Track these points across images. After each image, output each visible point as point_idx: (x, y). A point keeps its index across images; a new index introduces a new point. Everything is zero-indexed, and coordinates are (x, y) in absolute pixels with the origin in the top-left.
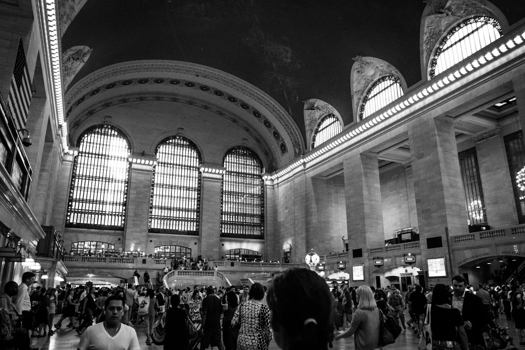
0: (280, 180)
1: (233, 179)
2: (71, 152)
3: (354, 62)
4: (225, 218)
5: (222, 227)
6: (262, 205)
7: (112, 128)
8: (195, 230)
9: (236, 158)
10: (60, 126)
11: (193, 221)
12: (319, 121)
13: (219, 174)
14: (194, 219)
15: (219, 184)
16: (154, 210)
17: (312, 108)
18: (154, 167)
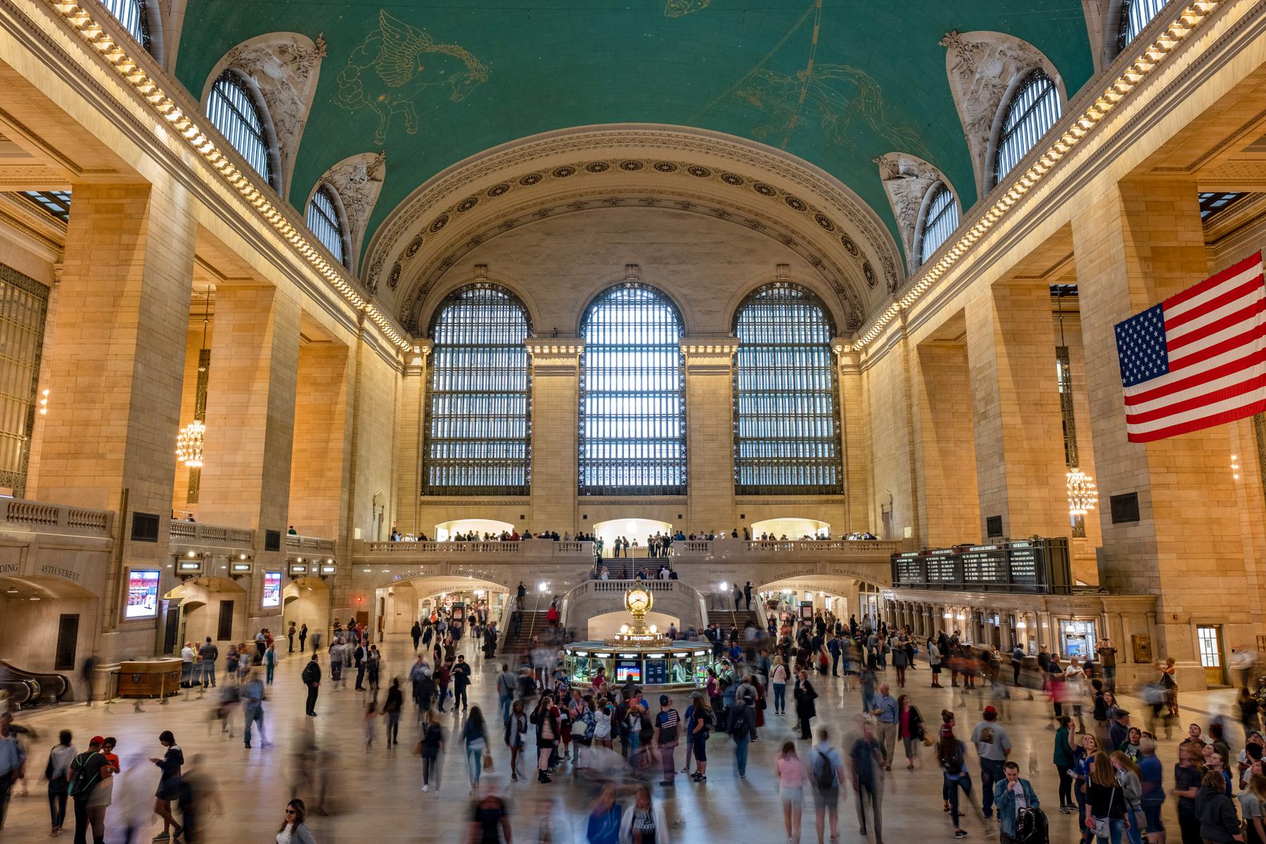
0: (871, 351)
1: (764, 359)
2: (417, 350)
3: (945, 49)
4: (747, 451)
5: (738, 473)
6: (837, 415)
7: (492, 287)
8: (677, 483)
10: (362, 314)
11: (673, 465)
12: (925, 202)
13: (722, 354)
14: (674, 458)
15: (727, 379)
16: (588, 447)
17: (896, 176)
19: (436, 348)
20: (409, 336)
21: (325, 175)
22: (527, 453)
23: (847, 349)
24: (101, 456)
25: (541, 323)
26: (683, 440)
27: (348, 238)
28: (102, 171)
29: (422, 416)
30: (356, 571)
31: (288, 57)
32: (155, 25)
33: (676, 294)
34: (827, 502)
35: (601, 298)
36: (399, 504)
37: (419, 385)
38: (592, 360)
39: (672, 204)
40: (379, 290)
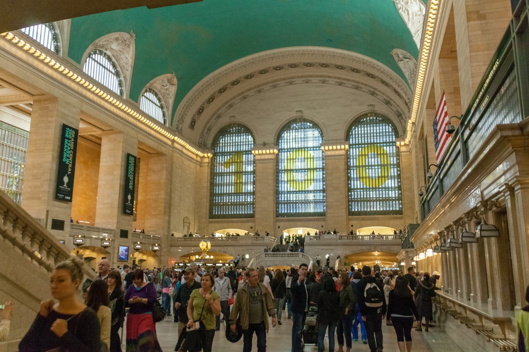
2: (206, 155)
9: (364, 128)
10: (173, 141)
18: (277, 155)
19: (215, 154)
20: (201, 149)
21: (148, 85)
22: (254, 199)
23: (402, 143)
24: (40, 199)
25: (260, 141)
26: (324, 191)
27: (165, 110)
28: (40, 95)
29: (209, 184)
30: (173, 249)
31: (120, 42)
32: (59, 39)
33: (320, 122)
34: (394, 218)
35: (287, 127)
36: (199, 223)
37: (207, 170)
38: (284, 155)
39: (317, 81)
40: (183, 129)
